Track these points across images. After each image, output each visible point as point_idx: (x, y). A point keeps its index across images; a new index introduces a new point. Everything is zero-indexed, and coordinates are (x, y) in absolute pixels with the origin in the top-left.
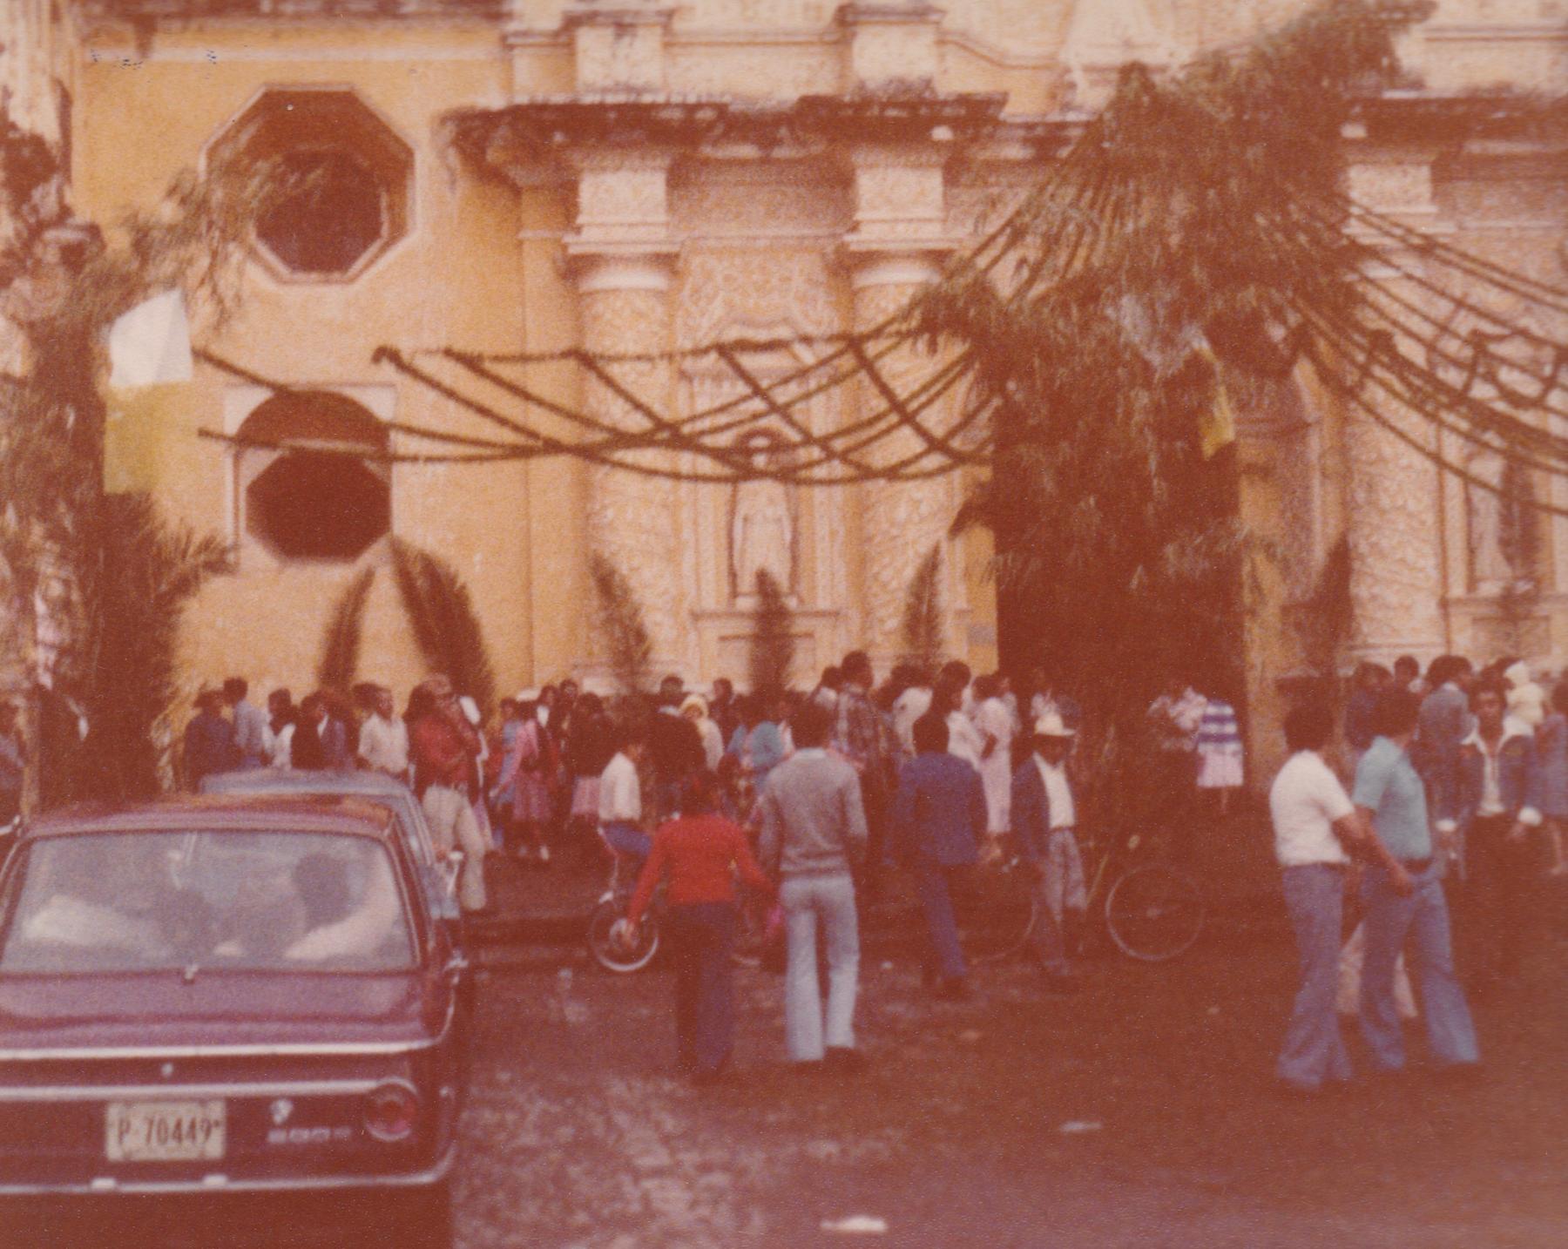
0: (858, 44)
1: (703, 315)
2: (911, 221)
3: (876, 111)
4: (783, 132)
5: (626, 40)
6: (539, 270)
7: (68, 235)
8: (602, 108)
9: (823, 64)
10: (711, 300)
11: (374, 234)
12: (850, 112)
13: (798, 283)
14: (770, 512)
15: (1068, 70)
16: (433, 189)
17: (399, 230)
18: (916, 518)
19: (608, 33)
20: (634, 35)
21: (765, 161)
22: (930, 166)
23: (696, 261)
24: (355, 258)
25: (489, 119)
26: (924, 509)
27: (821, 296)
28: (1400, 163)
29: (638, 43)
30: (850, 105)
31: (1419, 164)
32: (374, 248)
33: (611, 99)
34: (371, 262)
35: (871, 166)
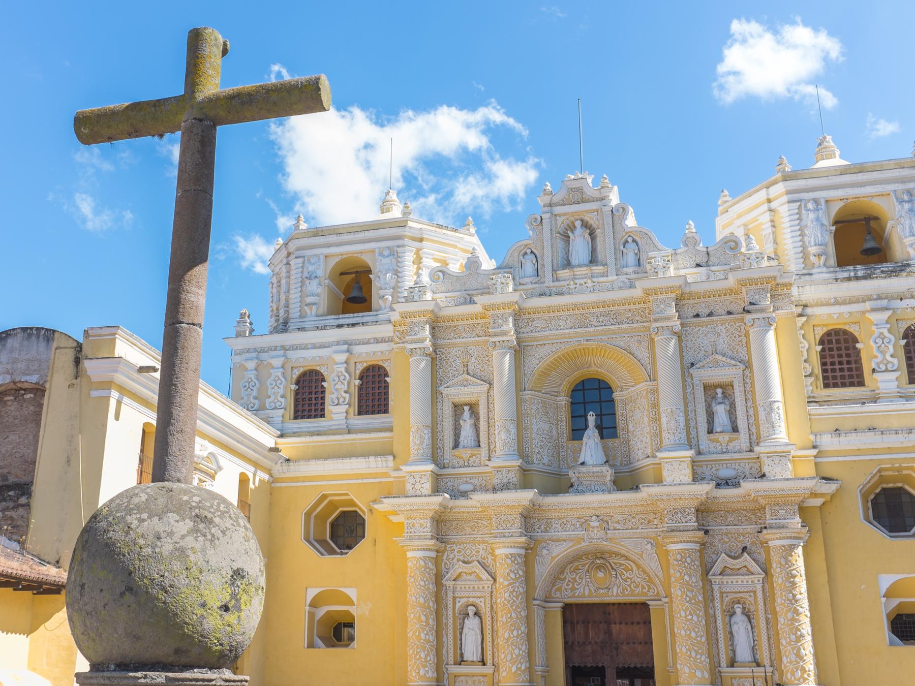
26: (515, 633)
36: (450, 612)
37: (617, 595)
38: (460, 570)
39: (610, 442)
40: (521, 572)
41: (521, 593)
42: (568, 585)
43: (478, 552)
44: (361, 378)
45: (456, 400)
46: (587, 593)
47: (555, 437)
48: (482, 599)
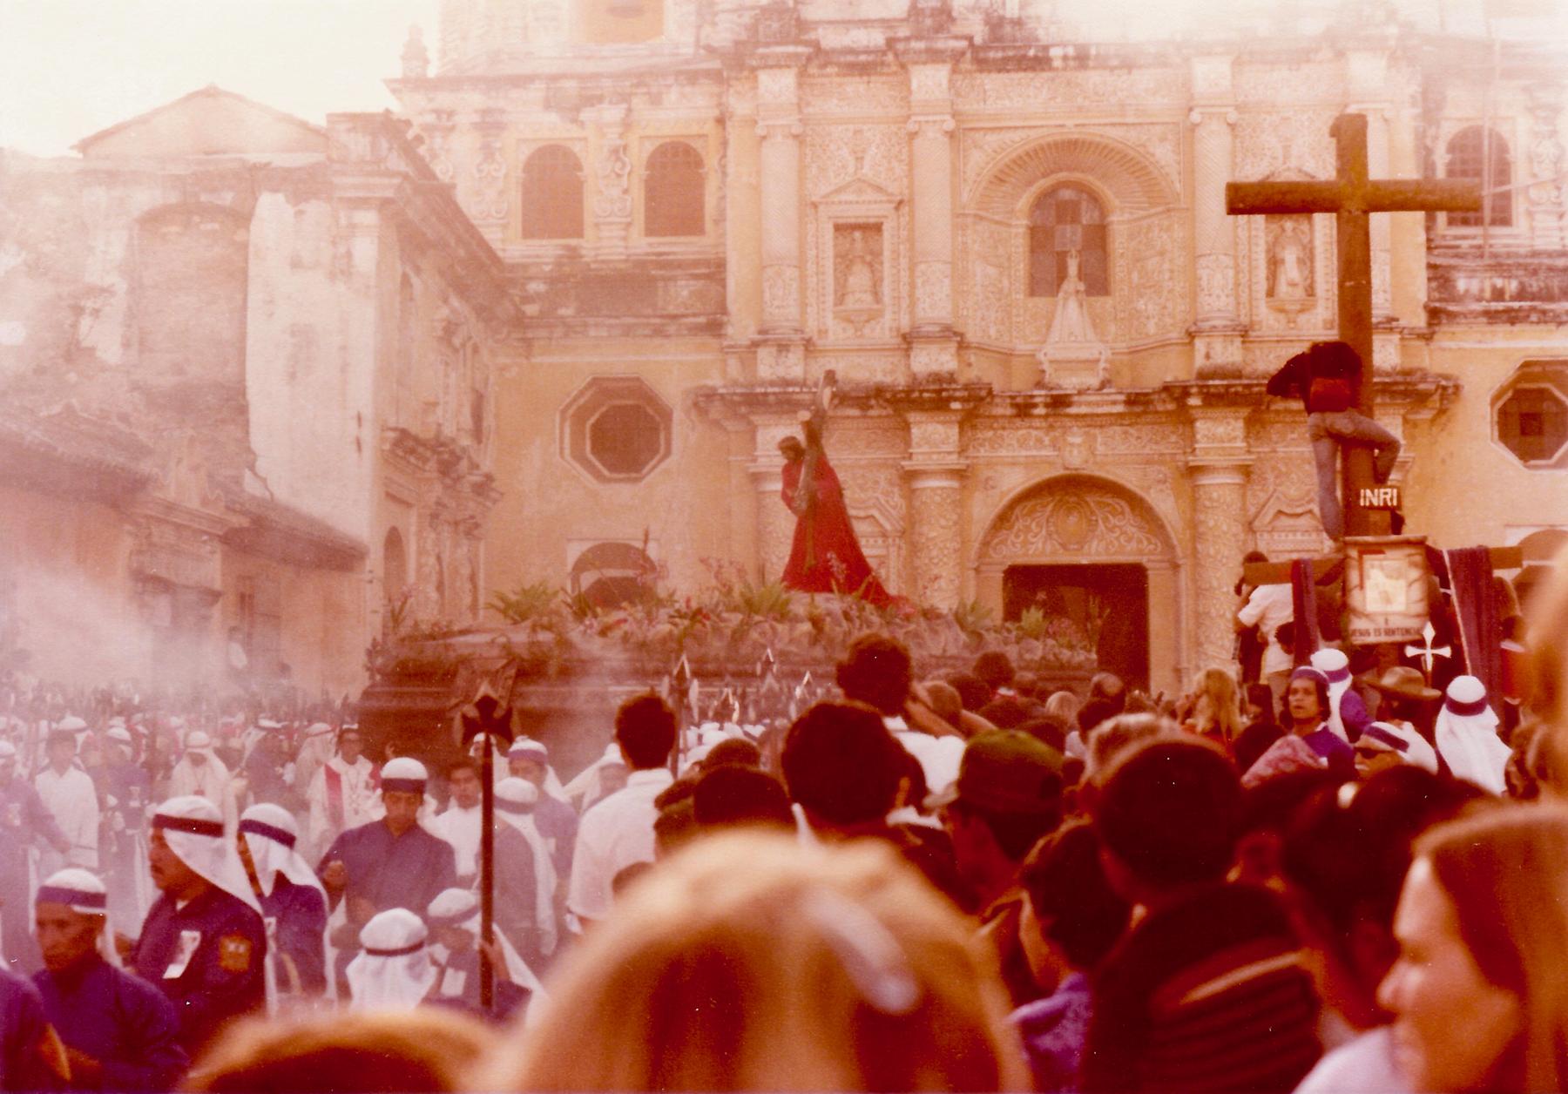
0: (913, 354)
3: (916, 394)
7: (476, 479)
8: (766, 394)
11: (656, 451)
13: (883, 484)
15: (1041, 363)
16: (684, 433)
17: (668, 453)
19: (774, 350)
21: (865, 417)
22: (951, 422)
25: (711, 395)
27: (896, 490)
31: (1237, 419)
32: (657, 458)
33: (770, 390)
34: (654, 467)
37: (1098, 553)
39: (1100, 302)
41: (955, 551)
42: (1017, 536)
43: (877, 482)
44: (651, 164)
45: (841, 221)
46: (1048, 548)
47: (1006, 291)
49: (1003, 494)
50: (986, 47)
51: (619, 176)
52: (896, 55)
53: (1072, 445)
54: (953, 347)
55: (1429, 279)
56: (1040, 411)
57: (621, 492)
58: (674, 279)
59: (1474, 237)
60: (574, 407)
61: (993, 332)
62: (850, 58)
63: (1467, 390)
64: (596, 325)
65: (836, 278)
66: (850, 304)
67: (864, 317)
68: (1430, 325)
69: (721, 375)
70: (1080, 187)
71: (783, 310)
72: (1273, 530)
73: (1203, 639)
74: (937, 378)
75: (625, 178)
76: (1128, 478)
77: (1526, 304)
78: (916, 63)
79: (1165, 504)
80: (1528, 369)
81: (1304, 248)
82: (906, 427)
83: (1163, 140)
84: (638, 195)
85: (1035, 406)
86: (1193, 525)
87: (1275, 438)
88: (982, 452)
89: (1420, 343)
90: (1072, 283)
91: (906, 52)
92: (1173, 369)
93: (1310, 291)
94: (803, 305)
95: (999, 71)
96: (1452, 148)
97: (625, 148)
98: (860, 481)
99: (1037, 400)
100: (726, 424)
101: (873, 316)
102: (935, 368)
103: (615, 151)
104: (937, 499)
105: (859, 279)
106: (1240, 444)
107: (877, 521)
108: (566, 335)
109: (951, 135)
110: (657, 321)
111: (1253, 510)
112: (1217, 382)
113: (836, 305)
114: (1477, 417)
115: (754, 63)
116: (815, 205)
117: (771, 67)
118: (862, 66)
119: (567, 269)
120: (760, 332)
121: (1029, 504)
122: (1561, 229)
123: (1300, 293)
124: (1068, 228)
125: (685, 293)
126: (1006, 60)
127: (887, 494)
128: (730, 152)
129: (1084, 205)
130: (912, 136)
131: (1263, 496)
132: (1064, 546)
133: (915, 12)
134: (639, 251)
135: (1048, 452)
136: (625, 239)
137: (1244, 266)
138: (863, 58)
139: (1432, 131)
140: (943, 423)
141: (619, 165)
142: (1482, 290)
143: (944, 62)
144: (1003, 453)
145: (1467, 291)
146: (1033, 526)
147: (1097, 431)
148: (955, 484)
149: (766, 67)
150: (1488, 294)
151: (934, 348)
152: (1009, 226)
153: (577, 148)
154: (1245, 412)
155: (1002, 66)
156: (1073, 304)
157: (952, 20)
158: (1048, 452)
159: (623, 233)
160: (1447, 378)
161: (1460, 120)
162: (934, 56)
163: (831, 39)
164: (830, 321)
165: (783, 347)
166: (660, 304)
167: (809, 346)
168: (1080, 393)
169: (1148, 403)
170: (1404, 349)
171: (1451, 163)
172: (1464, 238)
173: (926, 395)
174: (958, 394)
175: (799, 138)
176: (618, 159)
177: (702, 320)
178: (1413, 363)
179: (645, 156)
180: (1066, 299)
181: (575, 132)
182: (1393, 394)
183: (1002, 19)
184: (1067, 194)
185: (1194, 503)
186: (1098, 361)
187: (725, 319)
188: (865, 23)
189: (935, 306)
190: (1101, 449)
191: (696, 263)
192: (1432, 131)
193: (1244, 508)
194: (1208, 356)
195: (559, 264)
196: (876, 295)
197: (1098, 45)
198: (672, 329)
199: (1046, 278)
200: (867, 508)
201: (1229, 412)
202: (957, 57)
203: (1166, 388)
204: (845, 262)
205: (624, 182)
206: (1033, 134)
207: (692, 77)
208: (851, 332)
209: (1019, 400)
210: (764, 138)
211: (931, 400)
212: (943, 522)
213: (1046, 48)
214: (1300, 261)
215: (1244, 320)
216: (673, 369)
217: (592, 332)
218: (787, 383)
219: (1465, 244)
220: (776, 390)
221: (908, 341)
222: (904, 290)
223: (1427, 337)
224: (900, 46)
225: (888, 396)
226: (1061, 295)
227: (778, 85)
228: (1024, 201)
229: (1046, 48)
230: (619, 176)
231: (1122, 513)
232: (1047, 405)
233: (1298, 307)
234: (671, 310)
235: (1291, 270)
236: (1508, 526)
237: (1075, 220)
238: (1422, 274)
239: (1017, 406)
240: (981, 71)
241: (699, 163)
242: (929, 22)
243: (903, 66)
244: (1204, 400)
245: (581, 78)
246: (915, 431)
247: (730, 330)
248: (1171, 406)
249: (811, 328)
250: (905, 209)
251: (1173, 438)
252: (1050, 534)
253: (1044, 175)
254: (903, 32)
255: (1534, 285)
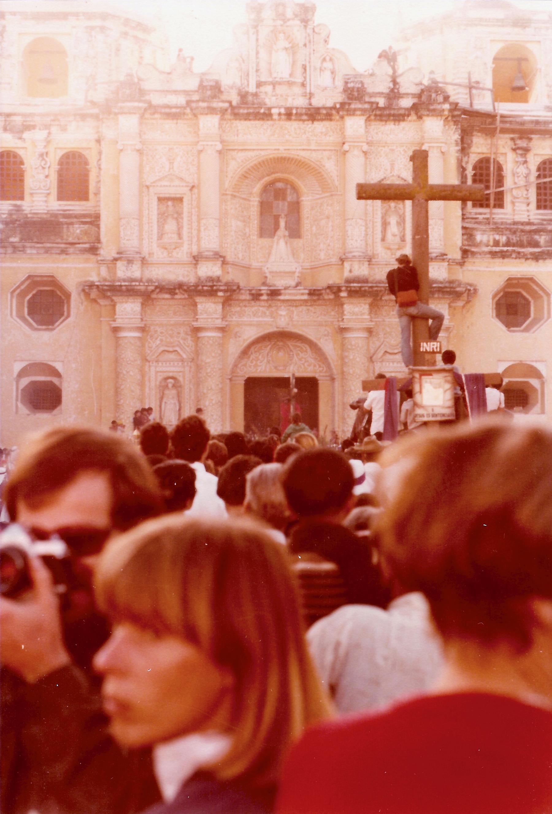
0: (198, 267)
1: (154, 343)
2: (212, 318)
3: (200, 288)
4: (177, 291)
5: (130, 265)
6: (105, 329)
8: (121, 286)
9: (192, 270)
10: (156, 339)
12: (193, 288)
13: (182, 335)
14: (172, 402)
15: (265, 273)
17: (69, 316)
18: (211, 404)
19: (125, 263)
20: (133, 263)
21: (172, 299)
23: (152, 328)
24: (57, 321)
25: (91, 285)
26: (214, 402)
27: (189, 338)
28: (359, 303)
29: (134, 266)
30: (193, 286)
31: (365, 304)
33: (123, 284)
35: (201, 302)
36: (153, 384)
38: (162, 349)
40: (219, 352)
41: (220, 369)
42: (252, 362)
43: (179, 333)
44: (61, 163)
45: (161, 196)
46: (268, 370)
47: (247, 234)
48: (181, 374)
49: (244, 340)
50: (238, 107)
51: (44, 168)
52: (192, 109)
53: (281, 315)
54: (219, 263)
55: (463, 235)
56: (265, 297)
57: (44, 336)
58: (72, 224)
59: (485, 214)
60: (18, 291)
61: (240, 256)
62: (167, 110)
63: (480, 292)
64: (31, 247)
65: (159, 226)
66: (166, 239)
67: (173, 247)
68: (463, 258)
69: (96, 274)
70: (286, 181)
71: (130, 242)
72: (382, 361)
73: (346, 416)
74: (211, 279)
75: (47, 170)
76: (310, 333)
77: (510, 249)
78: (202, 114)
79: (328, 347)
80: (511, 282)
81: (400, 216)
82: (195, 305)
83: (329, 159)
84: (54, 177)
85: (262, 295)
86: (342, 358)
87: (384, 314)
88: (234, 319)
89: (458, 267)
90: (282, 231)
91: (197, 108)
92: (333, 277)
93: (403, 239)
94: (141, 239)
95: (246, 119)
96: (475, 168)
97: (47, 153)
98: (170, 332)
99: (263, 292)
100: (99, 301)
101: (177, 246)
102: (210, 274)
103: (42, 155)
104: (211, 342)
105: (171, 226)
106: (367, 317)
107: (178, 353)
108: (14, 252)
109: (220, 152)
110: (63, 246)
111: (372, 351)
112: (355, 285)
113: (158, 240)
114: (485, 307)
115: (116, 111)
116: (148, 187)
117: (125, 113)
118: (173, 114)
119: (15, 217)
120: (118, 253)
121: (258, 346)
122: (528, 211)
123: (398, 239)
124: (281, 203)
125: (78, 231)
126: (249, 114)
127: (184, 339)
128: (103, 156)
129: (289, 191)
130: (200, 152)
131: (378, 344)
132: (276, 368)
133: (202, 87)
134: (53, 208)
135: (268, 319)
136: (46, 201)
137: (370, 225)
138: (174, 110)
139: (465, 159)
140: (215, 303)
141: (43, 162)
142: (489, 241)
143: (217, 114)
144: (245, 319)
145: (481, 241)
146: (260, 357)
147: (294, 308)
148: (219, 335)
149: (122, 113)
150: (491, 243)
151: (210, 264)
152: (249, 200)
153: (21, 153)
154: (369, 300)
155: (247, 117)
156: (282, 243)
157: (221, 92)
158: (268, 319)
159: (45, 199)
160: (471, 285)
161: (479, 153)
162: (212, 111)
163: (157, 100)
164: (155, 248)
165: (130, 262)
166: (65, 237)
167: (144, 261)
168: (286, 289)
169: (321, 294)
170: (450, 271)
171: (475, 175)
172: (481, 214)
173: (205, 288)
174: (222, 288)
175: (140, 152)
176: (43, 159)
177: (87, 246)
178: (453, 278)
179: (58, 158)
180: (278, 240)
181: (20, 144)
182: (443, 292)
183: (247, 93)
184: (280, 185)
185: (343, 347)
186: (294, 273)
187: (99, 245)
188: (175, 92)
189: (210, 241)
190: (296, 318)
191: (85, 216)
192: (465, 159)
193: (368, 350)
194: (351, 271)
195: (10, 214)
196: (180, 236)
197: (297, 108)
198: (71, 250)
199: (268, 230)
200: (173, 347)
201: (362, 300)
202: (223, 112)
203: (329, 287)
204: (163, 217)
205: (46, 172)
206: (263, 153)
207: (83, 117)
208: (165, 254)
209: (253, 292)
210: (121, 150)
211: (207, 291)
212: (213, 354)
213: (270, 109)
214: (398, 224)
215: (370, 253)
216: (72, 271)
217: (29, 251)
218: (132, 280)
219: (481, 217)
220: (127, 284)
221: (197, 259)
222: (195, 233)
223: (461, 264)
224: (194, 105)
225: (185, 288)
226: (276, 237)
227: (129, 123)
228: (258, 188)
229: (270, 109)
230: (44, 168)
231: (306, 351)
232: (268, 295)
233: (396, 247)
234: (71, 240)
235: (393, 228)
236: (499, 361)
237: (284, 199)
238: (460, 232)
239: (252, 295)
240: (236, 120)
241: (86, 163)
242: (209, 93)
243: (195, 115)
244: (348, 294)
245: (24, 115)
246: (199, 306)
247: (102, 252)
248: (332, 297)
249: (145, 252)
250: (195, 191)
251: (333, 313)
252: (268, 362)
253: (268, 175)
254: (195, 97)
255: (514, 239)
